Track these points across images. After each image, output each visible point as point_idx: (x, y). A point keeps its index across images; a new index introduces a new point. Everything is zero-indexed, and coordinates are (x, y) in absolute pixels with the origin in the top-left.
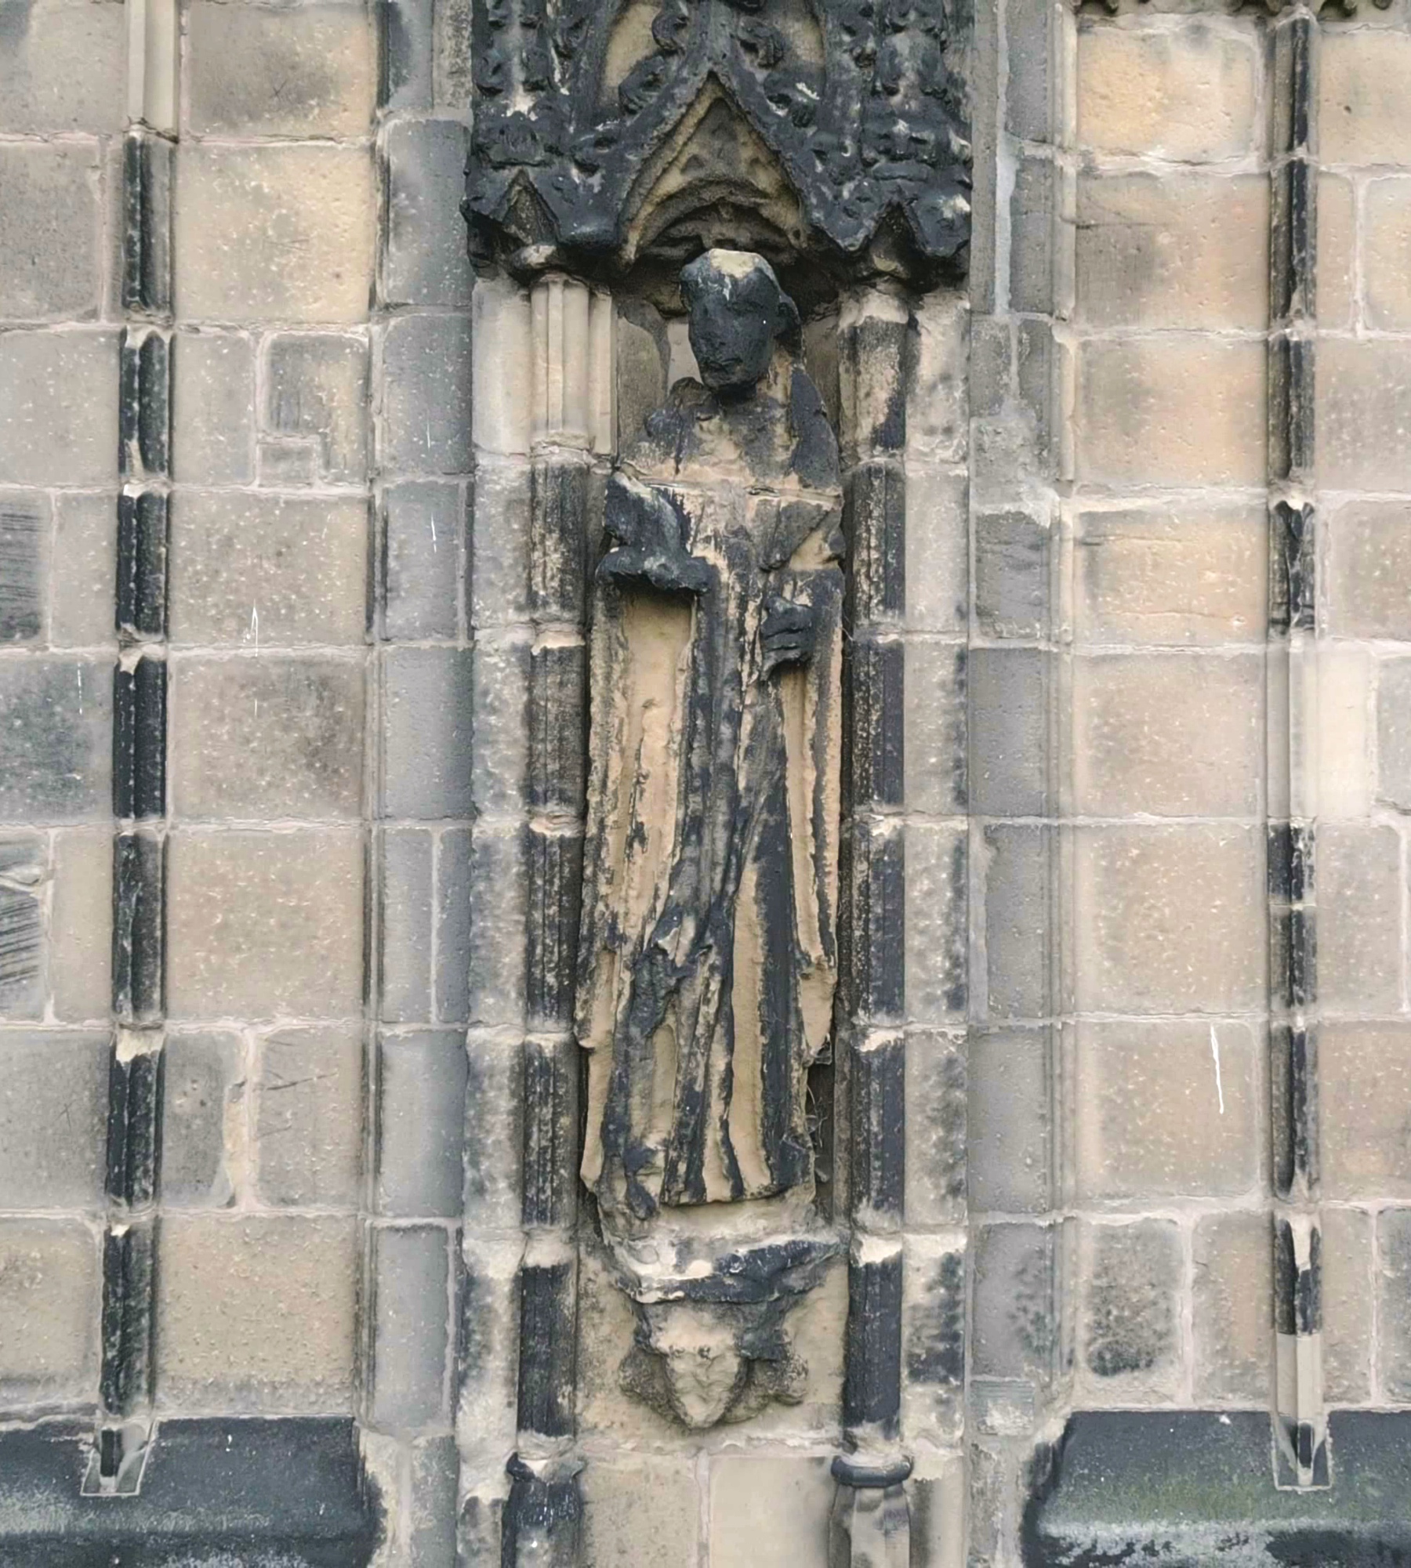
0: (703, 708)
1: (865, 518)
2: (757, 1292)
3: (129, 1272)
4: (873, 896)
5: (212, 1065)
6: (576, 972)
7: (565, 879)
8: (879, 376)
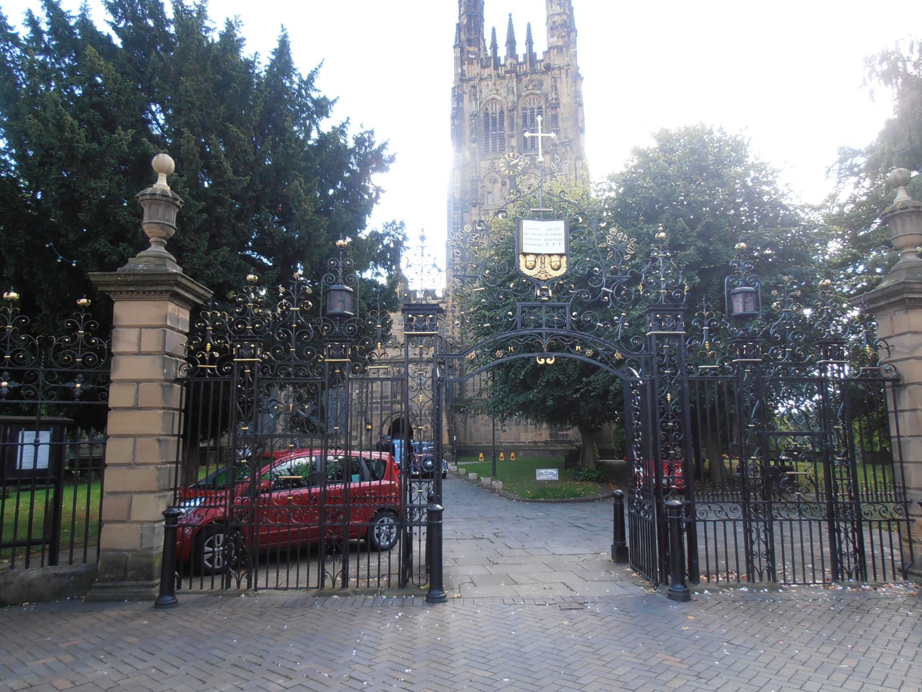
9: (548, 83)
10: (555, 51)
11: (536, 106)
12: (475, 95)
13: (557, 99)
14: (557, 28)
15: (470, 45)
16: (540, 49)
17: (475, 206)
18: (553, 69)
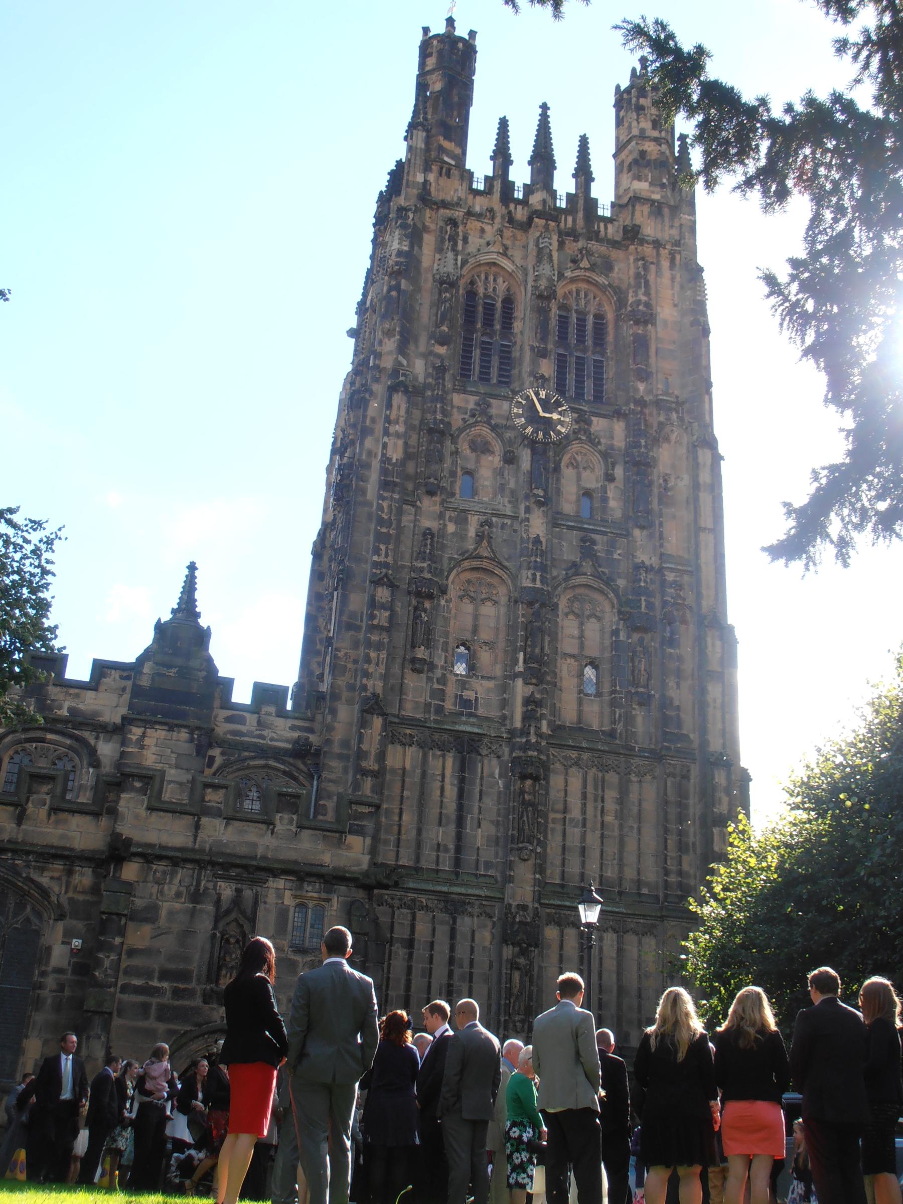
0: (521, 977)
1: (531, 964)
7: (509, 991)
9: (624, 267)
10: (646, 209)
11: (592, 309)
12: (453, 239)
13: (647, 305)
14: (648, 164)
15: (445, 138)
16: (604, 192)
17: (431, 493)
18: (642, 242)
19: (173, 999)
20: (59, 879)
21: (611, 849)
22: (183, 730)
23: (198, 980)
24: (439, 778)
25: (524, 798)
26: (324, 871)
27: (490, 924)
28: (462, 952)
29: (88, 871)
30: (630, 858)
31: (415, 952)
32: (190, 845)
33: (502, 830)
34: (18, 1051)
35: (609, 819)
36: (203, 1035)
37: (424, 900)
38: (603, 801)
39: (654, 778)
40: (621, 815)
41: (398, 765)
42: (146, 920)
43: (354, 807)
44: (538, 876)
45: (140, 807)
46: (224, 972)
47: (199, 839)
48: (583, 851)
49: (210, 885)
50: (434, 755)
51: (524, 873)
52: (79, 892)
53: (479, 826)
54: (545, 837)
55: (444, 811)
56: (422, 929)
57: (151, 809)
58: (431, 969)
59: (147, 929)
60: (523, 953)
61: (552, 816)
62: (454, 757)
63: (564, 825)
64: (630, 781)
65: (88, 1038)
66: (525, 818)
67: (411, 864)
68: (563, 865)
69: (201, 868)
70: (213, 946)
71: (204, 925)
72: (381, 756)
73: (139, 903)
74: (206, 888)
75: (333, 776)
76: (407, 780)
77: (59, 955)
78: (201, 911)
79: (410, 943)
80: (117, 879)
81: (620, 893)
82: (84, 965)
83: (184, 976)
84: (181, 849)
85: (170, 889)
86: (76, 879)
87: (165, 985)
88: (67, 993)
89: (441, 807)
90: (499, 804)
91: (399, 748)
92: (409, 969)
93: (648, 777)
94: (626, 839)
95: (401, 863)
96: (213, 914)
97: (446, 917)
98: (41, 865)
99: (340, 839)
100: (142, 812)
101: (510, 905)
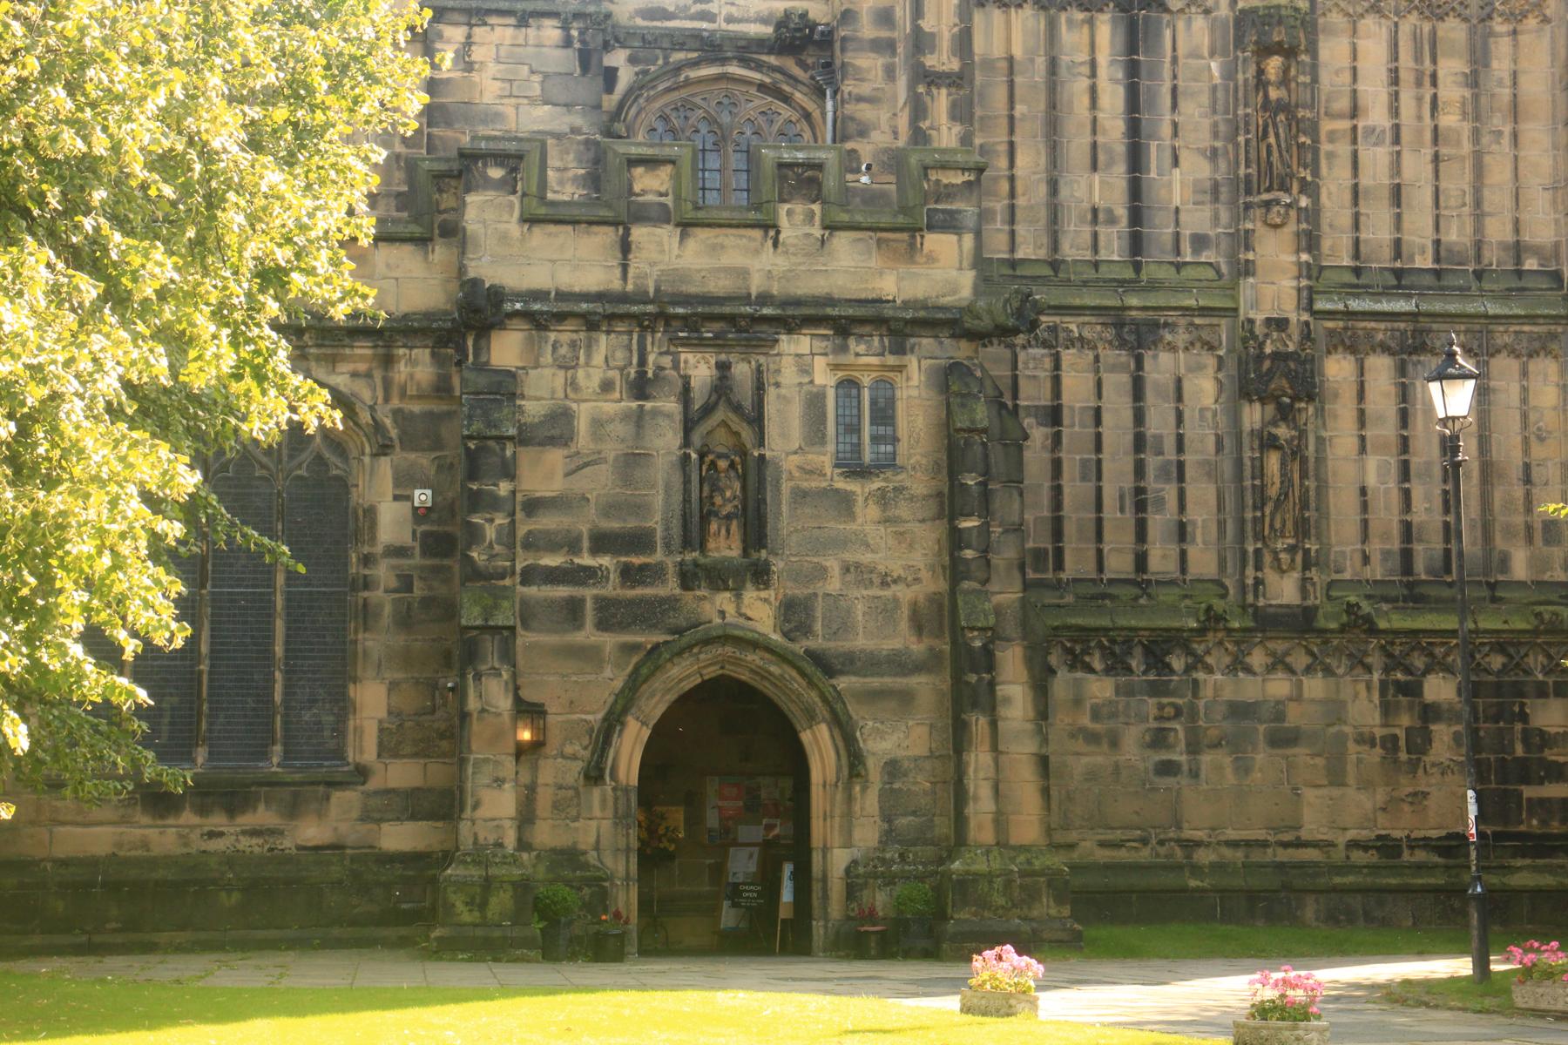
0: (1283, 464)
1: (1302, 434)
2: (1292, 550)
3: (1183, 555)
4: (1305, 492)
5: (1194, 523)
6: (1263, 505)
8: (1304, 415)
19: (623, 585)
20: (368, 375)
21: (1457, 182)
22: (548, 22)
23: (667, 545)
24: (1086, 70)
25: (1266, 96)
26: (888, 312)
27: (1210, 361)
28: (1159, 421)
29: (423, 355)
30: (1497, 198)
31: (1065, 431)
32: (616, 285)
33: (1223, 165)
34: (343, 707)
35: (1450, 120)
36: (690, 647)
37: (1073, 327)
38: (1434, 84)
39: (1546, 20)
40: (1475, 112)
41: (998, 51)
42: (552, 441)
43: (933, 176)
44: (1305, 257)
45: (506, 217)
46: (714, 527)
47: (631, 272)
48: (1396, 194)
49: (666, 361)
50: (1070, 22)
51: (1276, 253)
52: (412, 397)
53: (1176, 162)
54: (1316, 173)
55: (1100, 139)
56: (1076, 388)
57: (530, 220)
58: (1099, 462)
59: (555, 457)
60: (1285, 414)
61: (1326, 126)
62: (1114, 21)
63: (1354, 141)
64: (1492, 34)
65: (478, 677)
66: (1272, 140)
67: (1042, 254)
68: (1356, 226)
69: (644, 329)
70: (687, 482)
71: (666, 441)
72: (964, 41)
73: (533, 409)
74: (661, 368)
75: (865, 89)
76: (1018, 80)
77: (392, 522)
78: (656, 413)
79: (1054, 415)
80: (482, 367)
81: (1479, 275)
82: (442, 537)
83: (639, 541)
84: (600, 297)
85: (588, 376)
86: (402, 371)
87: (605, 561)
88: (419, 590)
89: (1094, 132)
90: (1214, 112)
91: (997, 15)
92: (1057, 466)
93: (1532, 22)
94: (1487, 159)
95: (1020, 255)
96: (678, 417)
97: (1123, 356)
98: (329, 351)
99: (912, 246)
100: (514, 228)
101: (1251, 321)
